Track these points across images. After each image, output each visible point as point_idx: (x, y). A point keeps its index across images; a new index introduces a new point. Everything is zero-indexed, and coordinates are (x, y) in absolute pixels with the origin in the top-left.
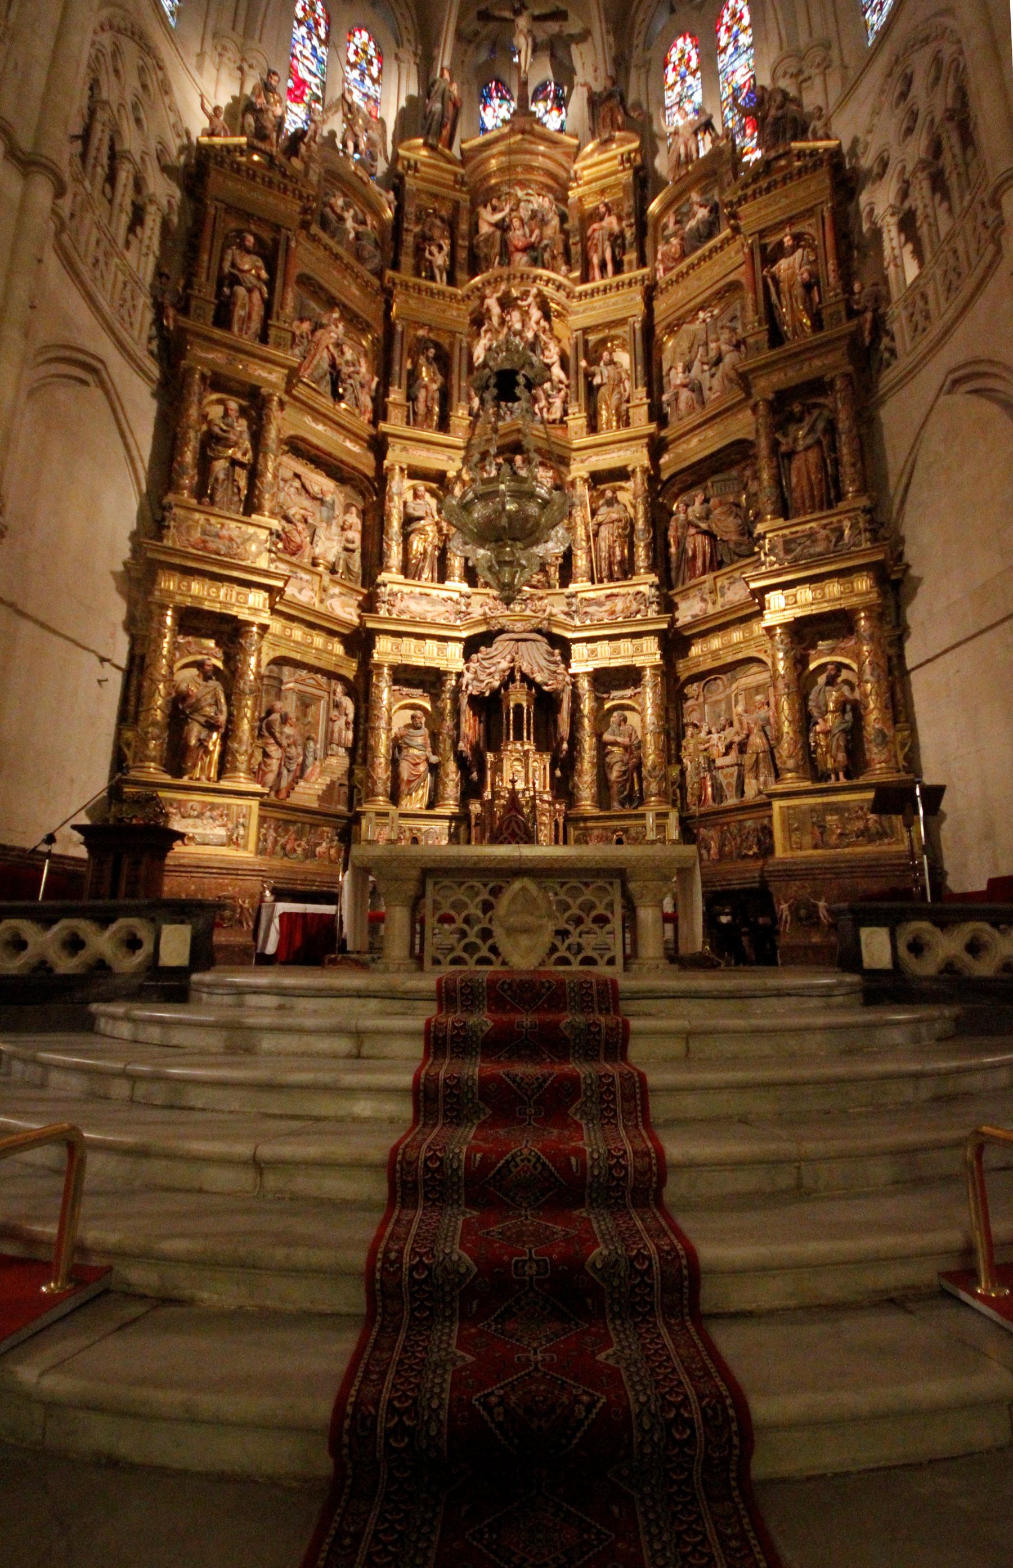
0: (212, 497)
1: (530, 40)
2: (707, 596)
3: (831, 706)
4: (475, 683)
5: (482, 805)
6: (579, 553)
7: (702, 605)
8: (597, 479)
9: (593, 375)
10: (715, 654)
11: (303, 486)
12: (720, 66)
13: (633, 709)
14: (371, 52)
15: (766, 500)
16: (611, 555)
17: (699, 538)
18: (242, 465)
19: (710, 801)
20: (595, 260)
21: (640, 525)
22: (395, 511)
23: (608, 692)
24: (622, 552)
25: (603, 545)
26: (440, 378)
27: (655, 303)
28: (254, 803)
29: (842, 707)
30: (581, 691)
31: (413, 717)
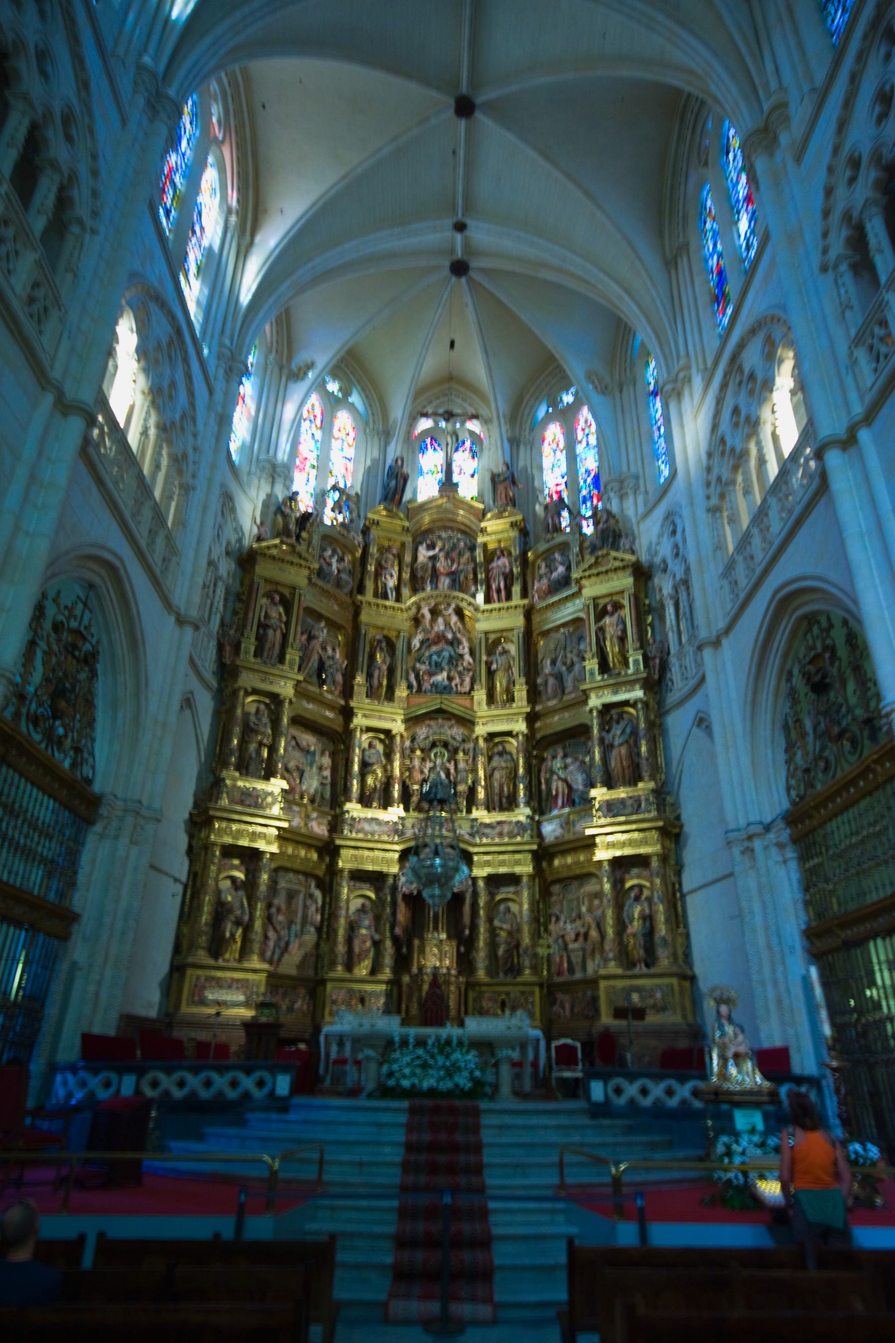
0: (247, 769)
1: (454, 439)
3: (636, 916)
5: (411, 977)
8: (491, 736)
9: (491, 663)
10: (569, 867)
11: (297, 744)
15: (597, 774)
17: (560, 783)
18: (265, 745)
19: (566, 973)
20: (494, 587)
21: (521, 771)
22: (356, 759)
23: (498, 888)
25: (496, 784)
26: (388, 660)
27: (533, 617)
28: (262, 977)
31: (363, 905)
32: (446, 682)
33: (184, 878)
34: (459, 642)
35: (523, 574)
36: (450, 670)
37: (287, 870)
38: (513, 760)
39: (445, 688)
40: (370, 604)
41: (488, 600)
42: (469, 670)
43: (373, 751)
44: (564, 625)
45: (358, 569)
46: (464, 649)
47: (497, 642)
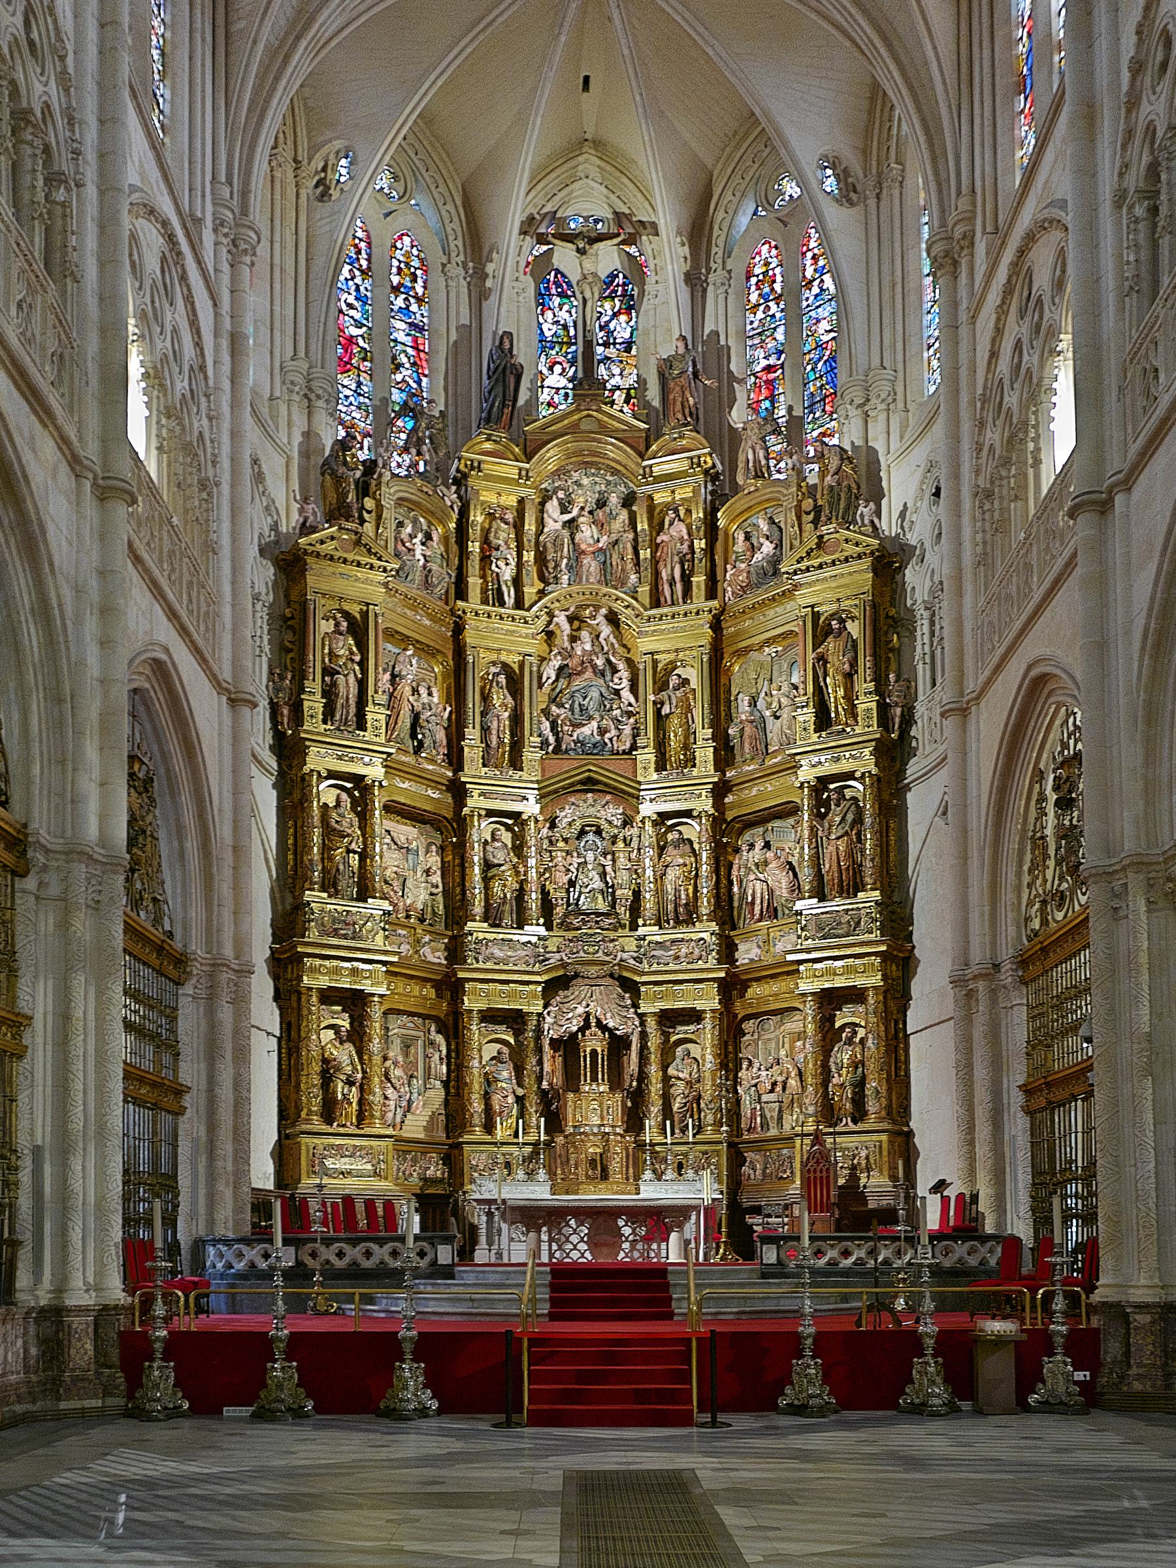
2: (761, 944)
4: (556, 1027)
6: (648, 896)
7: (759, 951)
8: (663, 816)
9: (662, 704)
12: (805, 304)
13: (696, 1043)
14: (415, 263)
16: (677, 897)
17: (758, 884)
22: (476, 859)
24: (687, 895)
29: (855, 1064)
30: (649, 1030)
32: (599, 738)
33: (278, 1034)
34: (615, 670)
35: (710, 550)
36: (602, 718)
37: (399, 1012)
38: (693, 850)
39: (595, 746)
40: (477, 614)
41: (656, 602)
42: (630, 714)
43: (497, 844)
44: (768, 642)
45: (454, 548)
46: (622, 681)
47: (671, 667)
